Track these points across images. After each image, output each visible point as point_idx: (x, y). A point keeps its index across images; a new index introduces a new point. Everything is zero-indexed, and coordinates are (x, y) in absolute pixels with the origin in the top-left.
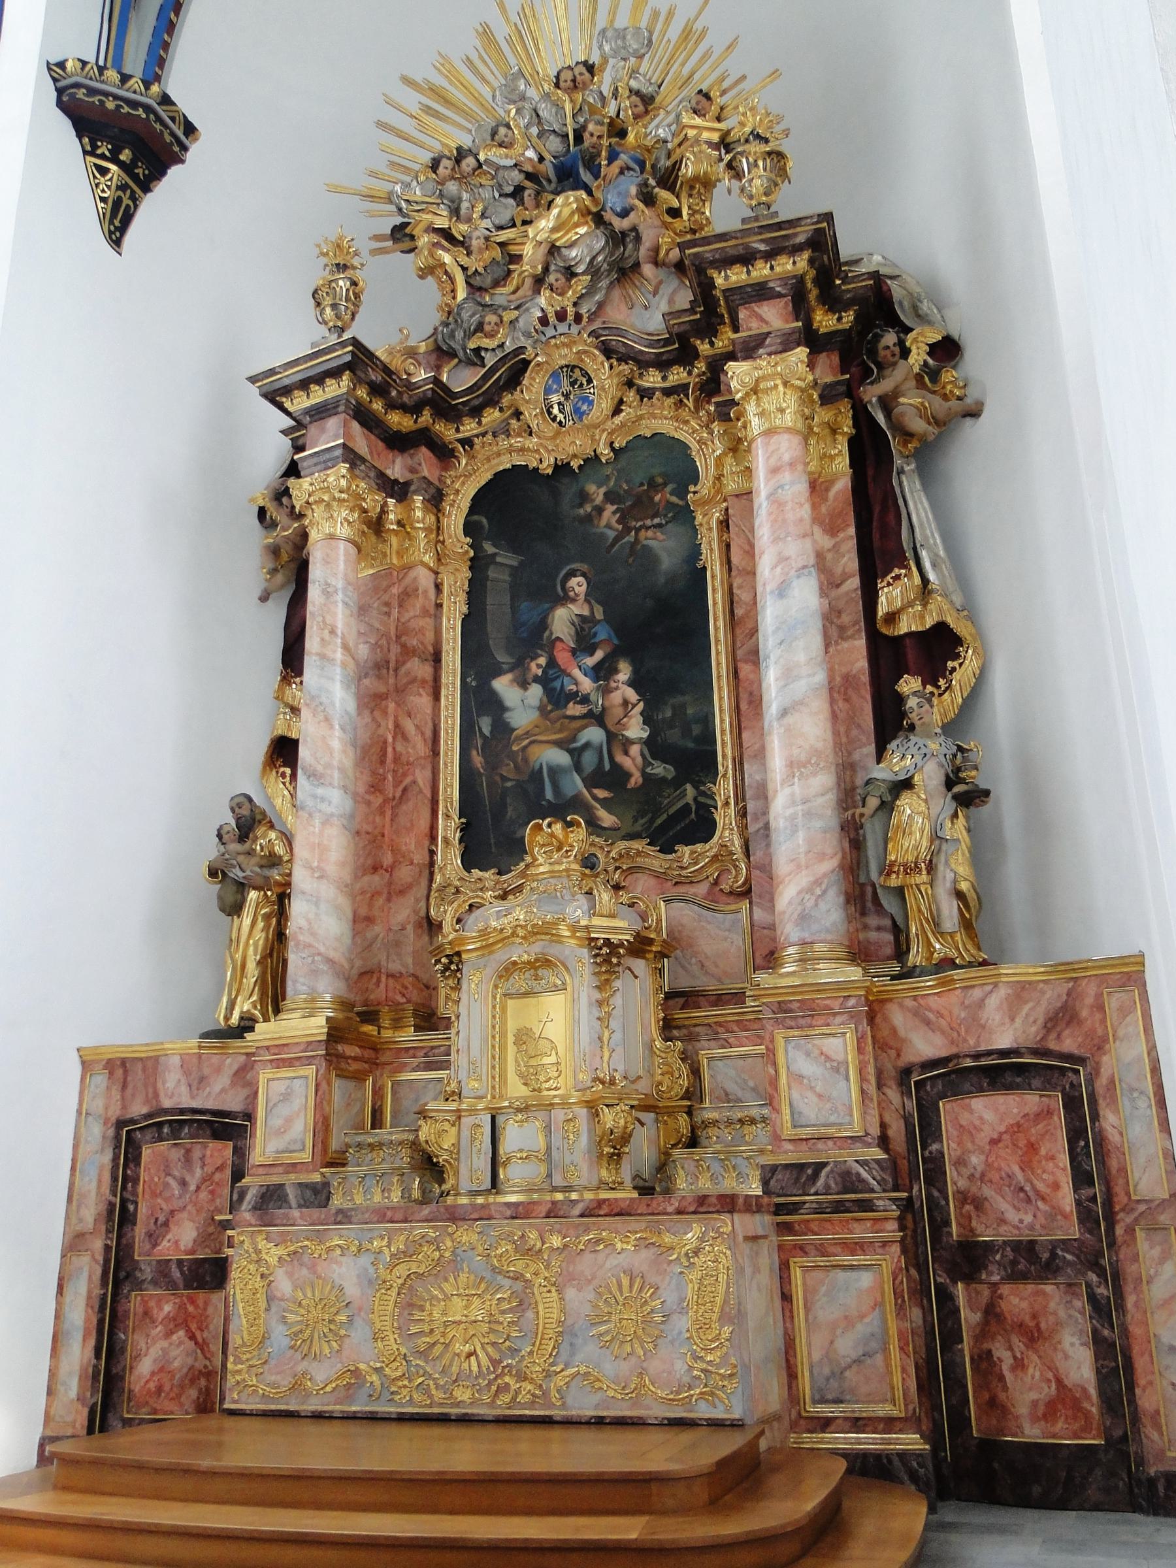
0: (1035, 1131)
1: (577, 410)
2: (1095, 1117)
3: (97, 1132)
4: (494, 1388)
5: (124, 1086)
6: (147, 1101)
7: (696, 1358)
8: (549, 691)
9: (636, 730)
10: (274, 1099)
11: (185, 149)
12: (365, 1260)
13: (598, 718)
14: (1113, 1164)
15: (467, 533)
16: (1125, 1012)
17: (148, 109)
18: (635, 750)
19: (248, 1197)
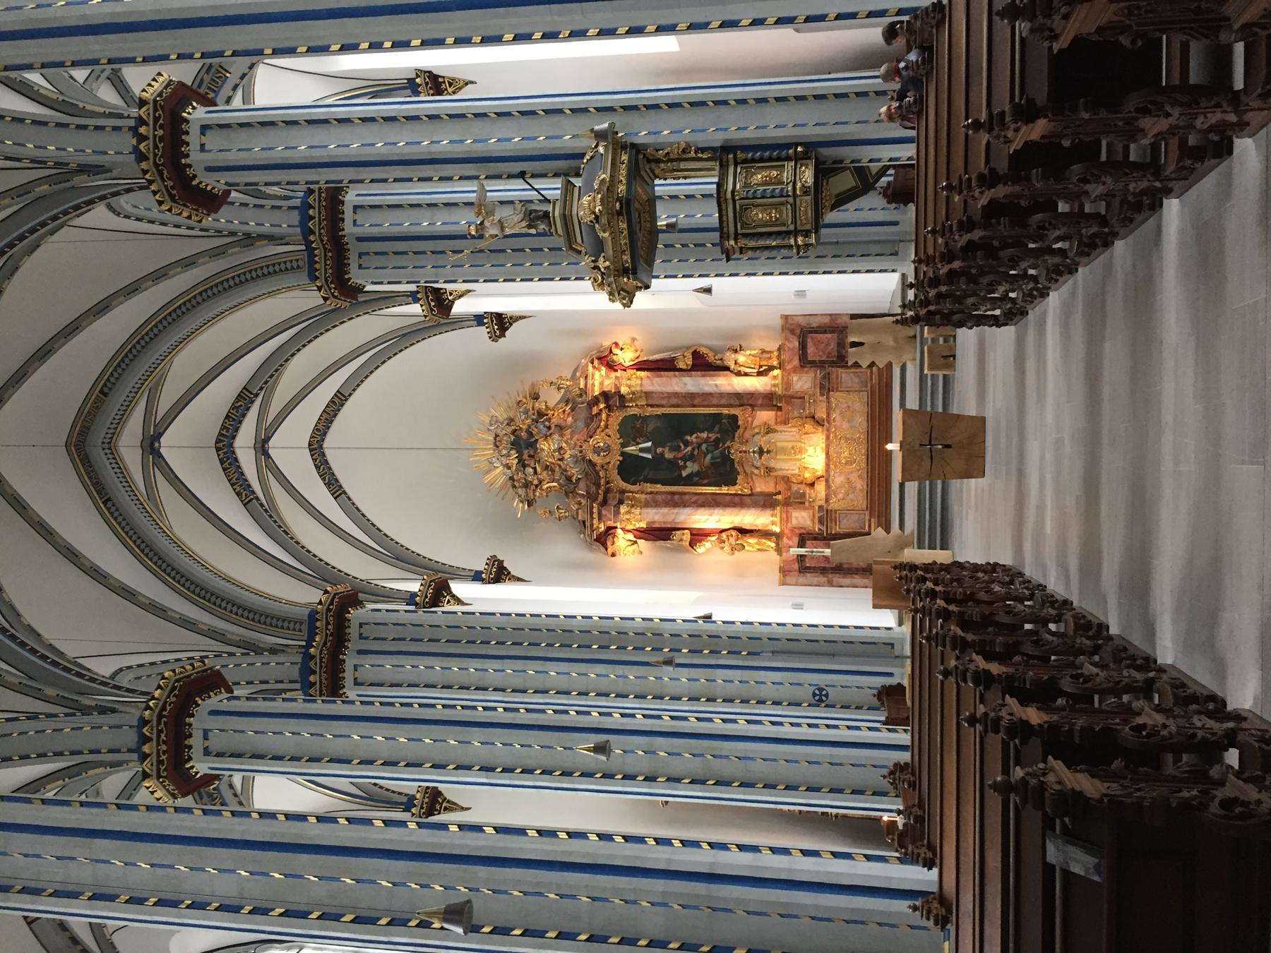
3: (802, 579)
9: (704, 435)
12: (836, 475)
13: (699, 445)
16: (793, 320)
17: (494, 561)
18: (710, 435)
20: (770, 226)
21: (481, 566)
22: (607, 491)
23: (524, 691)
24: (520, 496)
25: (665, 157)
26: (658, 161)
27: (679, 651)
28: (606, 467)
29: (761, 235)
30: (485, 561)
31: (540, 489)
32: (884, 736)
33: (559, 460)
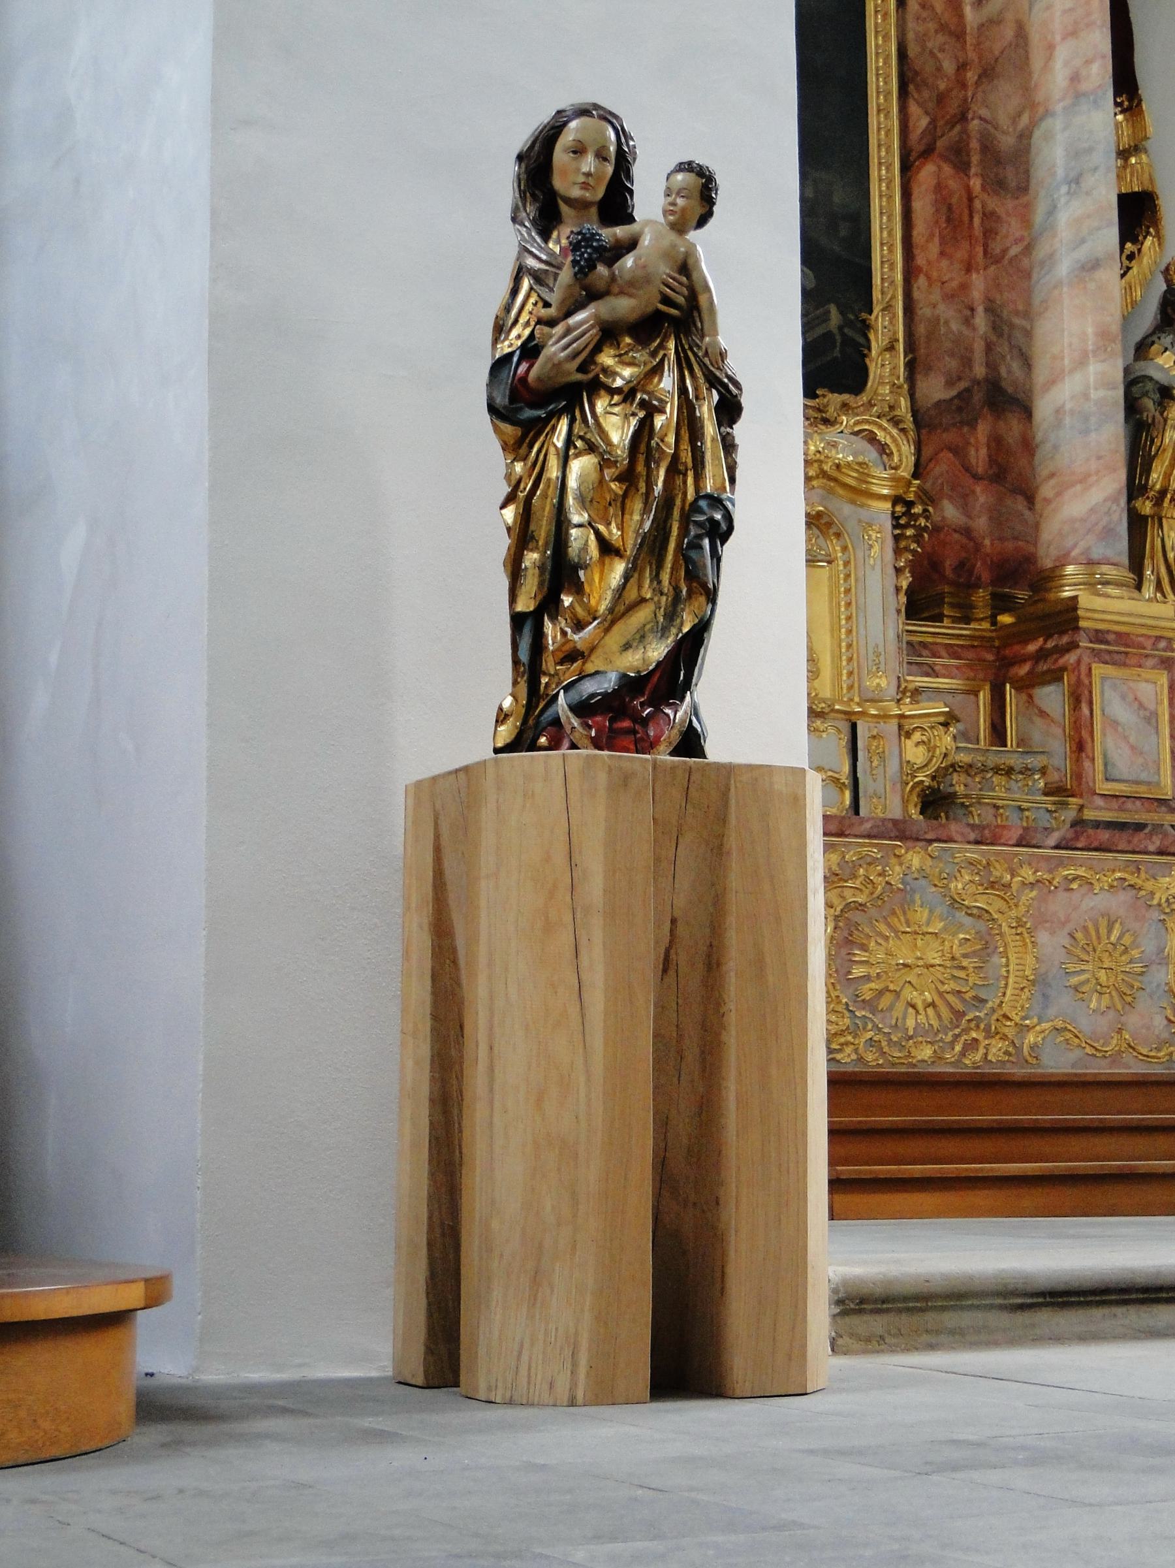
4: (958, 1048)
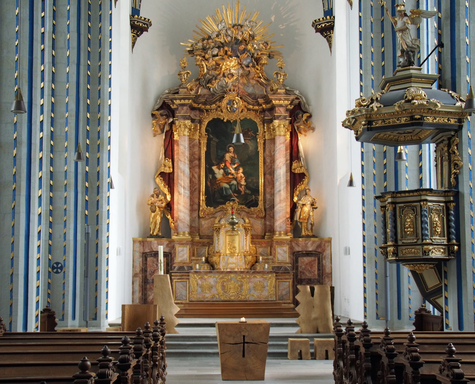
0: (313, 263)
1: (233, 110)
2: (322, 261)
3: (137, 255)
5: (143, 246)
6: (149, 249)
7: (269, 292)
8: (225, 171)
9: (243, 183)
10: (180, 251)
11: (148, 28)
12: (214, 279)
14: (324, 268)
15: (206, 132)
16: (328, 246)
17: (147, 25)
18: (243, 187)
19: (176, 268)
20: (401, 228)
21: (143, 14)
22: (201, 110)
23: (53, 48)
24: (196, 44)
25: (452, 151)
26: (449, 146)
27: (87, 165)
28: (219, 109)
29: (395, 221)
30: (147, 18)
31: (202, 60)
32: (33, 312)
33: (224, 74)
